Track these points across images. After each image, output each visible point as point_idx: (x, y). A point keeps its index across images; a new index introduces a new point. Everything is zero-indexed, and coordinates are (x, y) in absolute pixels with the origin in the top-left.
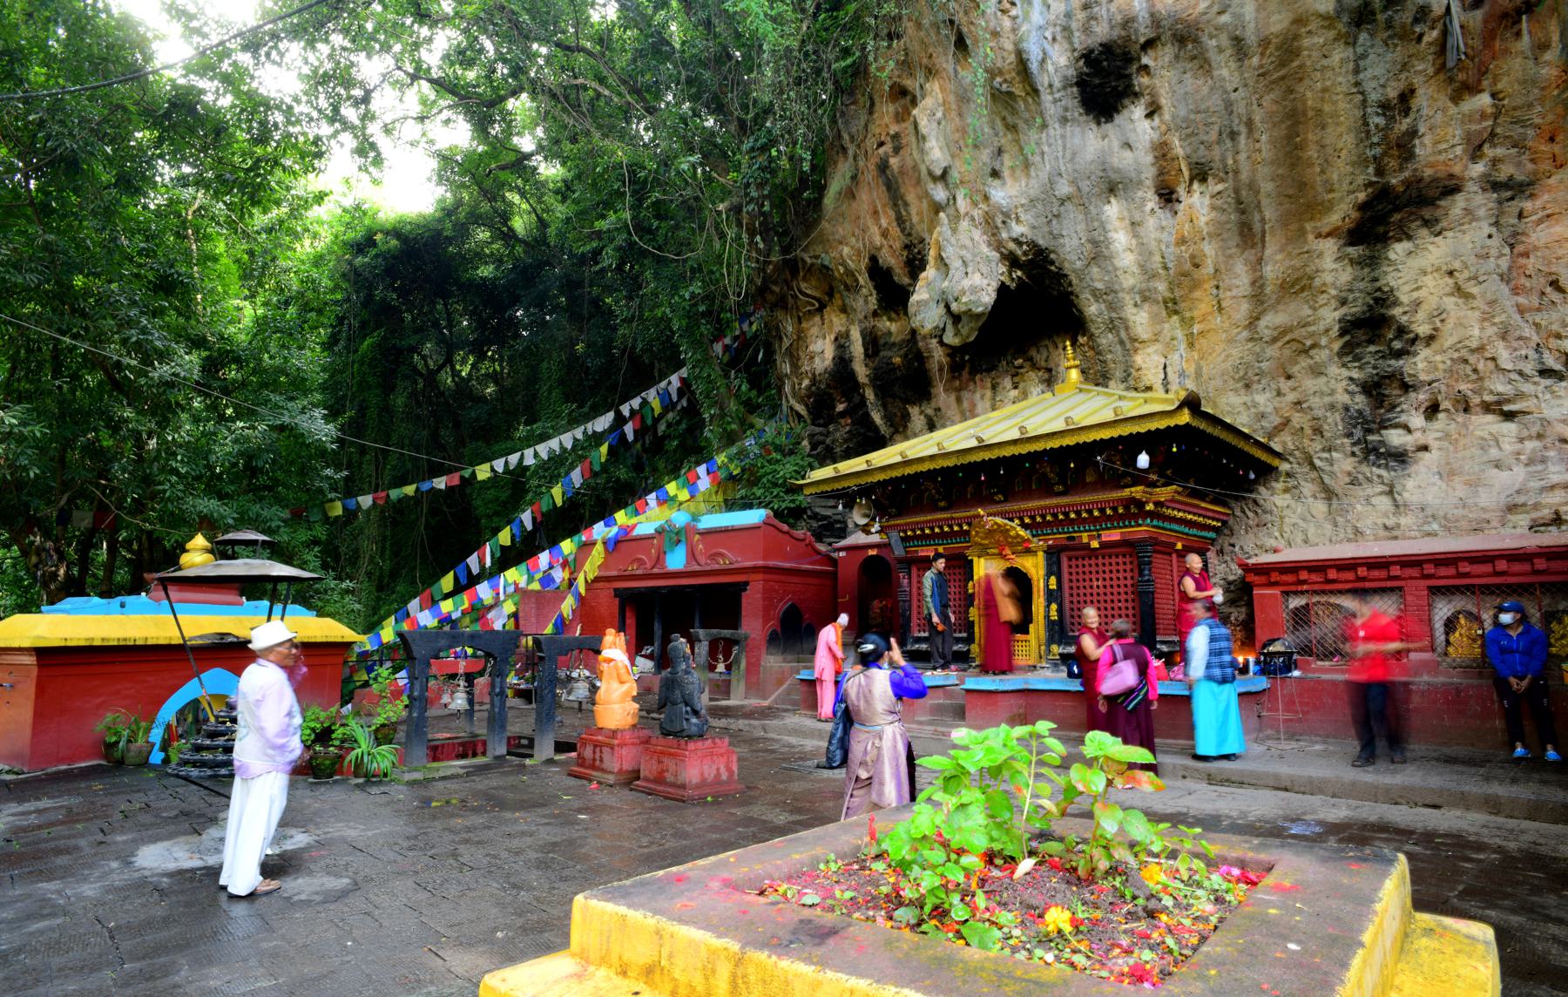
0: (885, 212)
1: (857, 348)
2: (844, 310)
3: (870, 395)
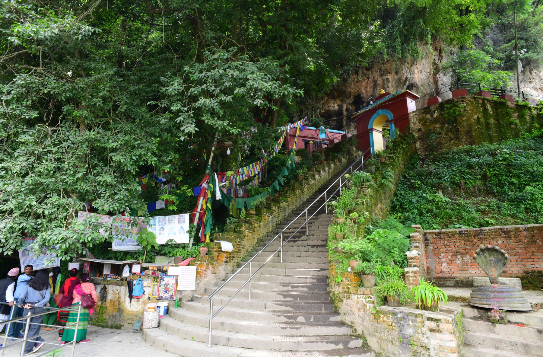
0: (370, 88)
1: (344, 109)
2: (342, 101)
3: (345, 118)
